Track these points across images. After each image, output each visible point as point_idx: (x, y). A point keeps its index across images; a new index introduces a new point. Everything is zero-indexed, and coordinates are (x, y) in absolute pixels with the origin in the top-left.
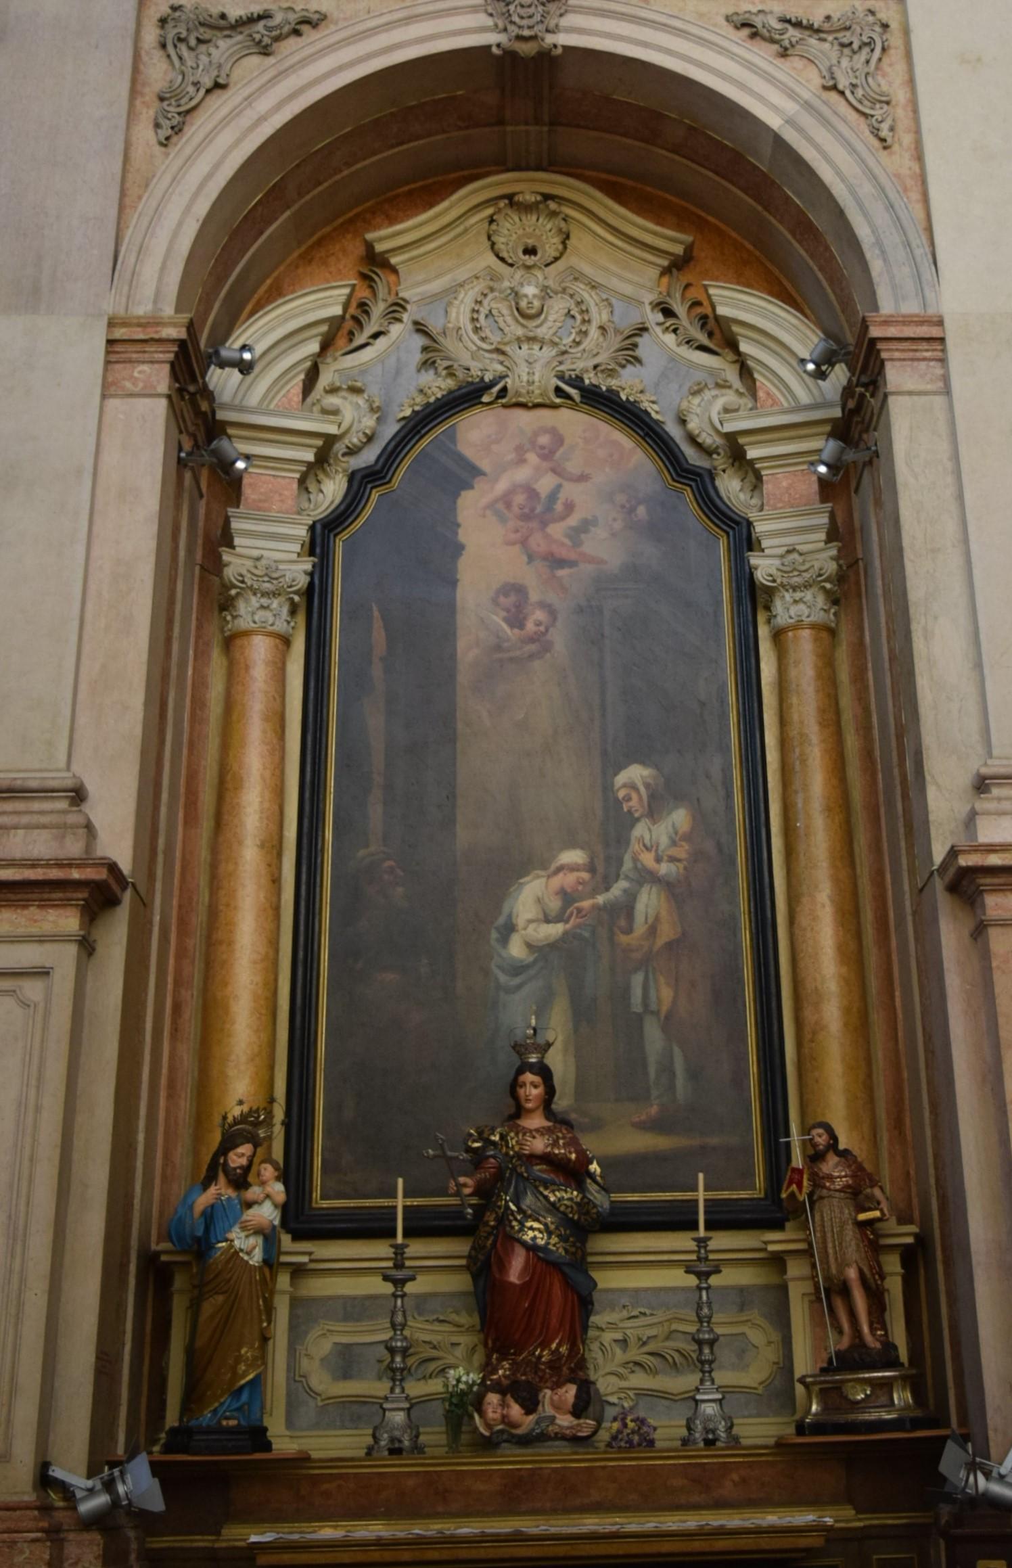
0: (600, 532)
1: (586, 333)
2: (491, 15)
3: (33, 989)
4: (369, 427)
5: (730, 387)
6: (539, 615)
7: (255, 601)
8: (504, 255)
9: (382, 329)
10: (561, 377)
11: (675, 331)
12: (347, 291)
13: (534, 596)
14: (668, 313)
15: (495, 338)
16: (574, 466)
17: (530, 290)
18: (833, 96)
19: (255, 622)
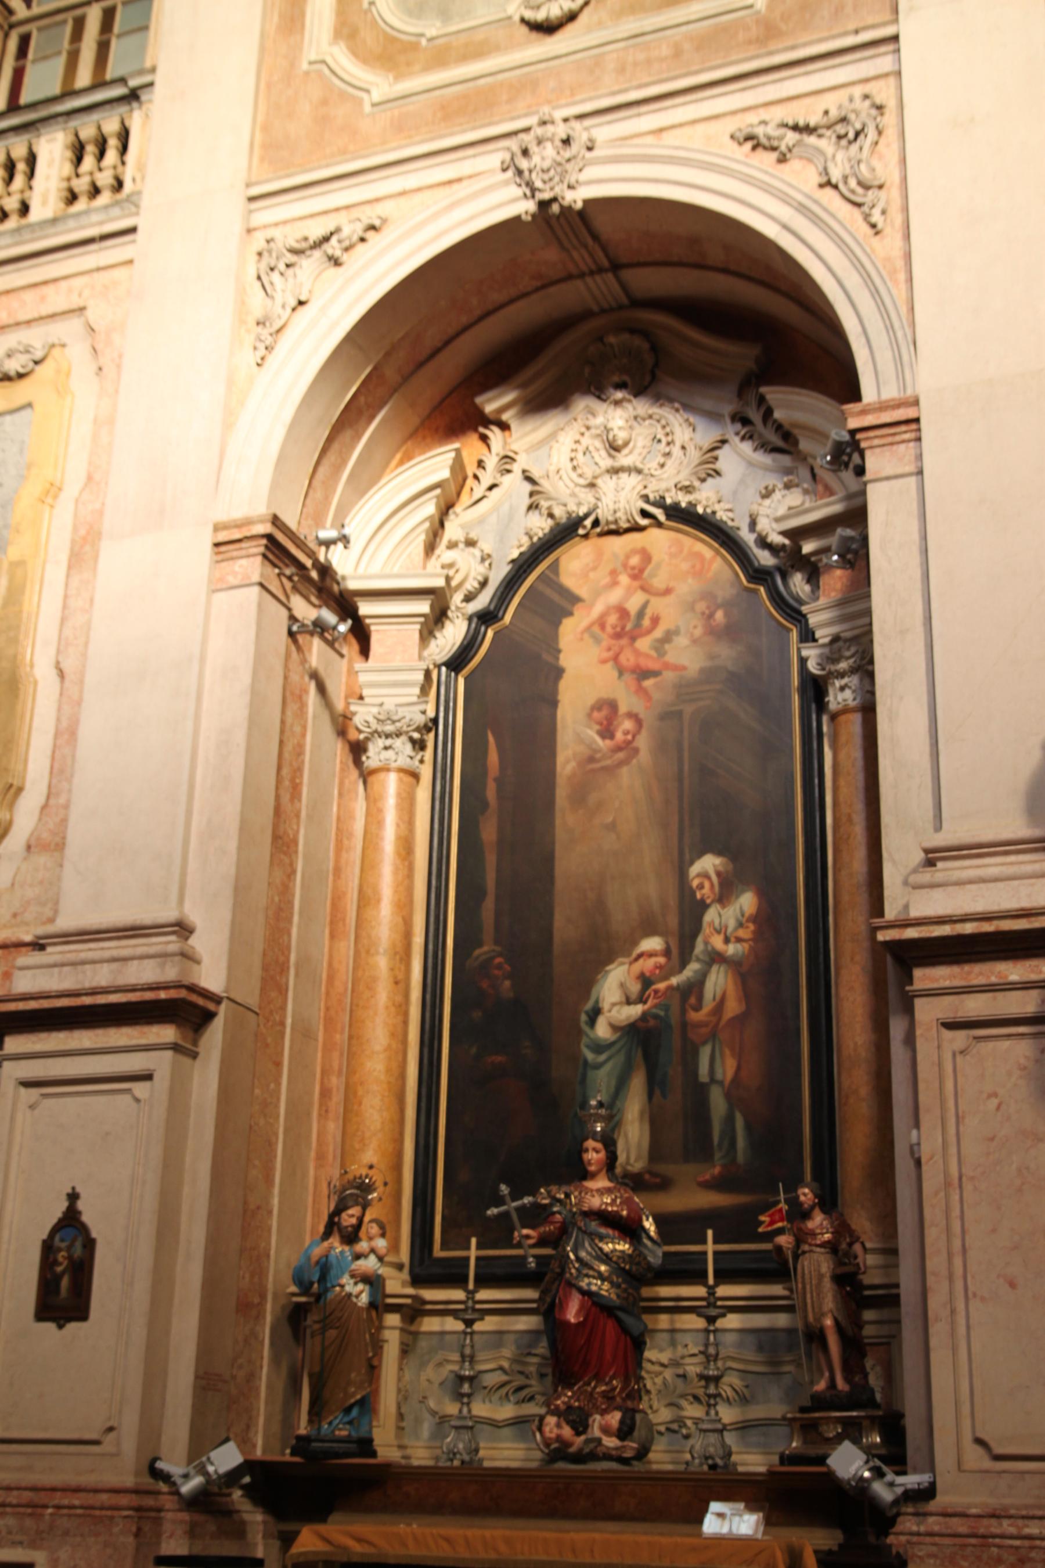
0: (682, 641)
2: (520, 185)
3: (140, 1089)
4: (480, 574)
6: (628, 725)
7: (381, 742)
9: (496, 482)
12: (453, 454)
13: (623, 709)
15: (589, 472)
16: (658, 582)
18: (829, 191)
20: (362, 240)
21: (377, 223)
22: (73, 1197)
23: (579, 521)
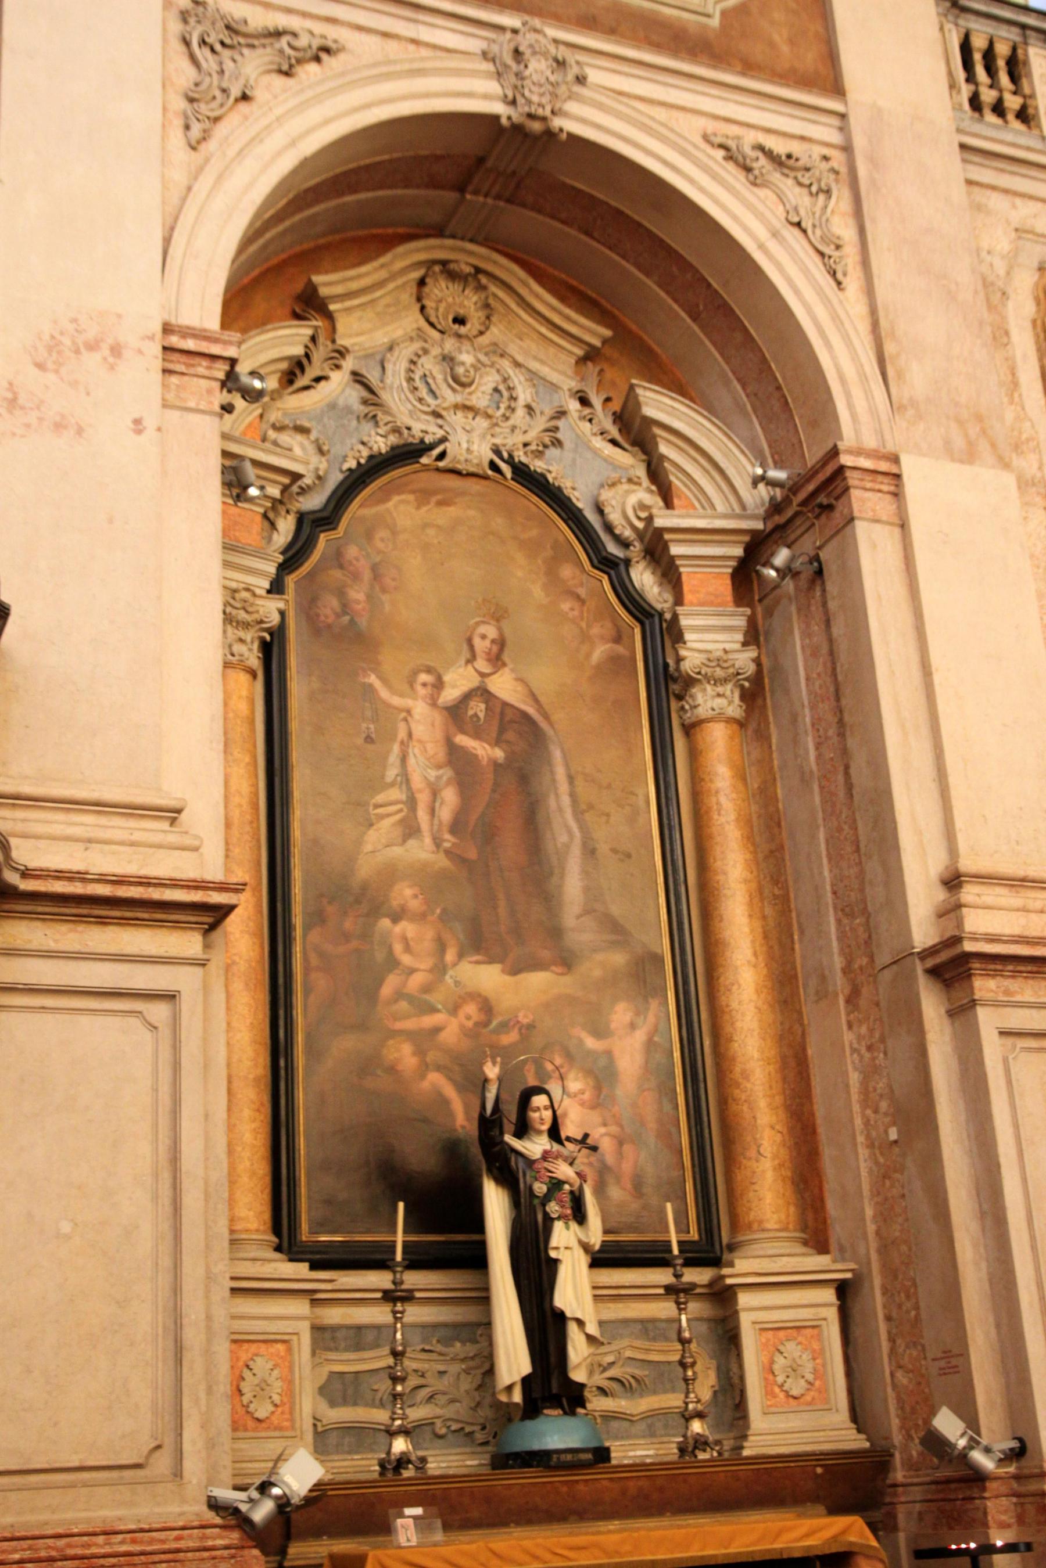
1: (513, 410)
5: (640, 484)
8: (433, 319)
10: (497, 452)
11: (590, 420)
14: (584, 401)
17: (467, 358)
19: (233, 655)
20: (317, 59)
21: (334, 46)
23: (420, 449)
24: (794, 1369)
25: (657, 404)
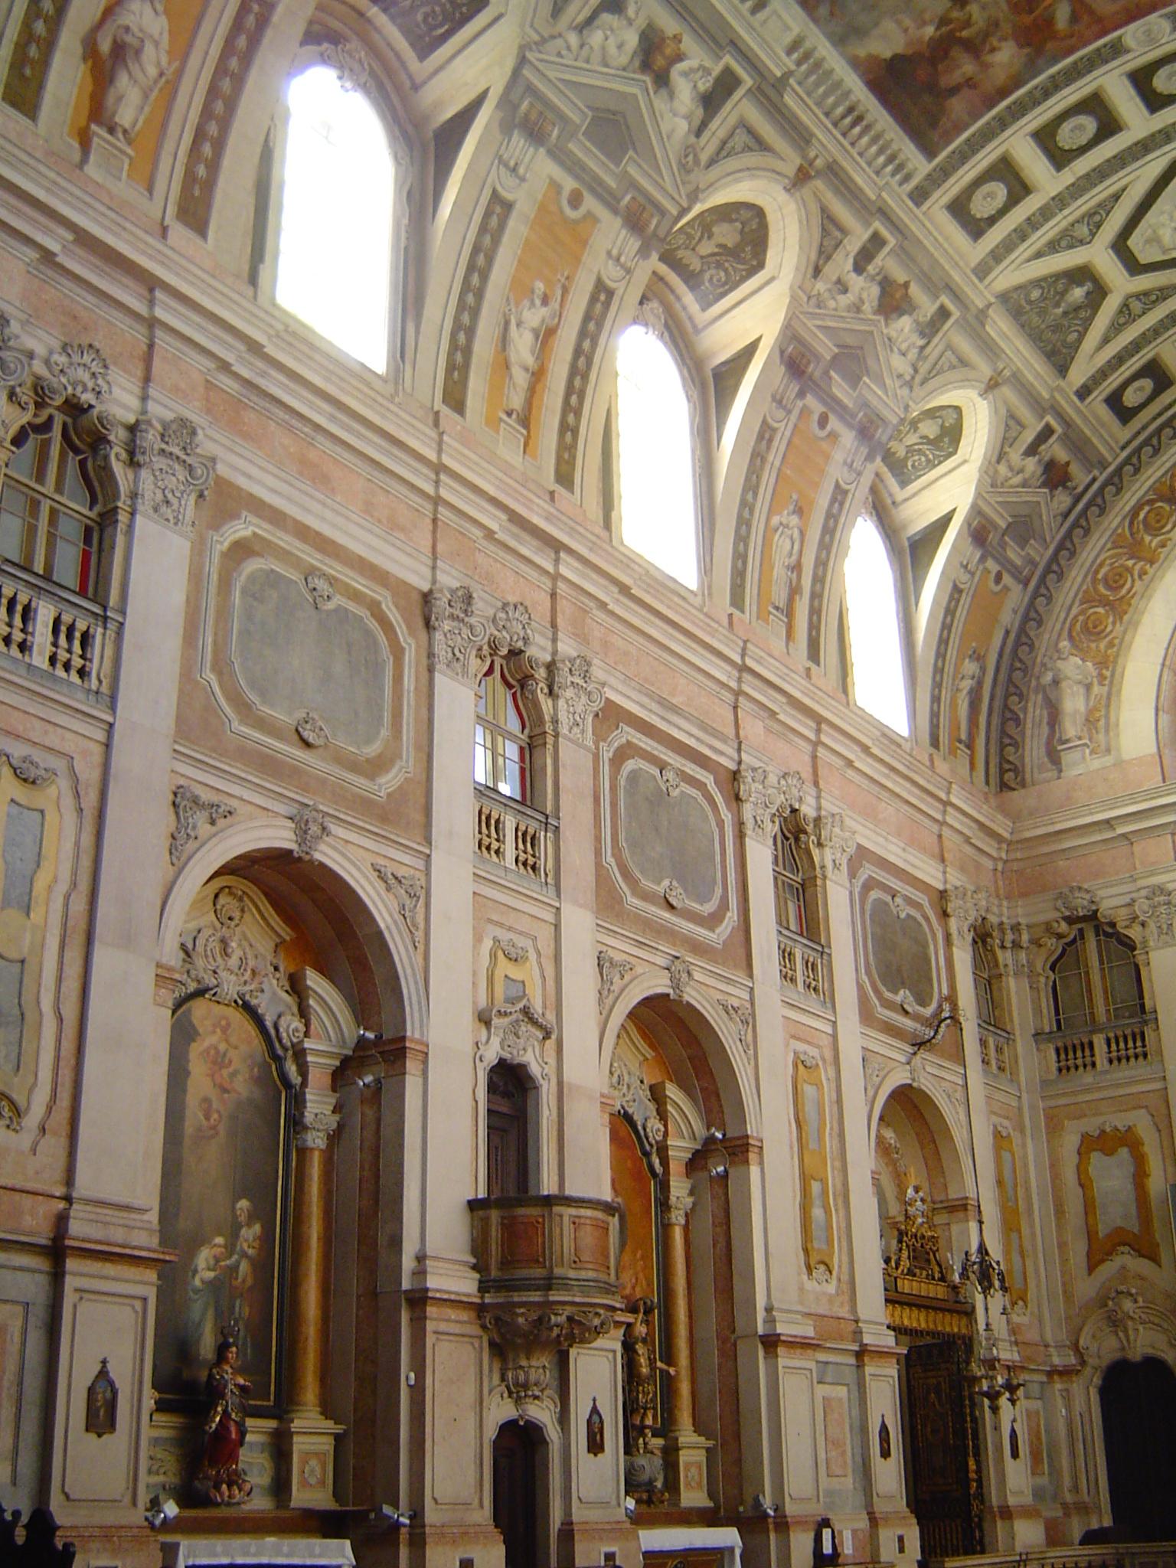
0: (240, 1078)
6: (215, 1116)
13: (214, 1106)
16: (233, 1040)
22: (104, 1362)
24: (312, 1471)
25: (314, 980)
